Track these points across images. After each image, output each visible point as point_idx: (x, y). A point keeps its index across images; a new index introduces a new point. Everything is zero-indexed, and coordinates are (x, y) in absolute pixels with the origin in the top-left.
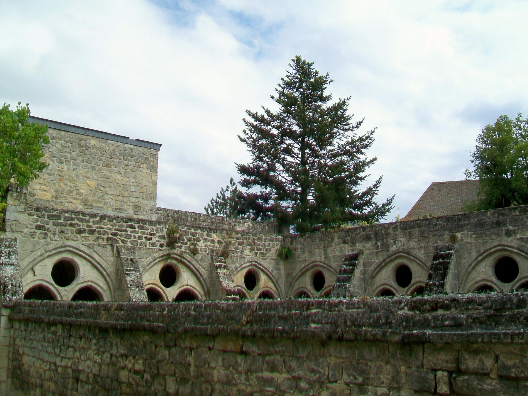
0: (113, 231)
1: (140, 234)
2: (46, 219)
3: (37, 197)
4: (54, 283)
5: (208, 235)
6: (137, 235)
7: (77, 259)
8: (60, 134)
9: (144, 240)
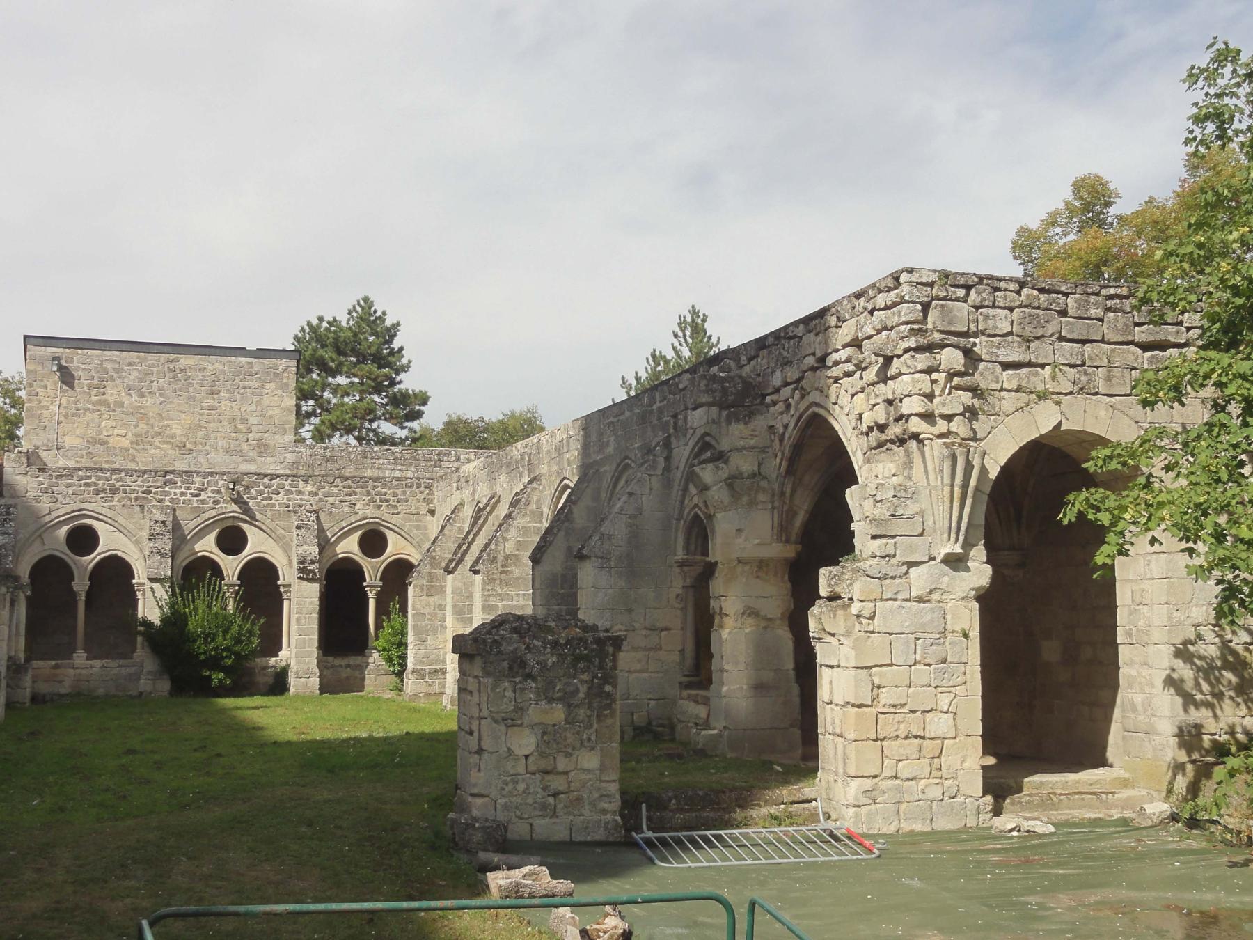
0: (145, 488)
1: (183, 490)
2: (54, 480)
3: (109, 445)
4: (68, 552)
5: (291, 485)
6: (178, 491)
7: (95, 524)
8: (138, 357)
9: (189, 497)
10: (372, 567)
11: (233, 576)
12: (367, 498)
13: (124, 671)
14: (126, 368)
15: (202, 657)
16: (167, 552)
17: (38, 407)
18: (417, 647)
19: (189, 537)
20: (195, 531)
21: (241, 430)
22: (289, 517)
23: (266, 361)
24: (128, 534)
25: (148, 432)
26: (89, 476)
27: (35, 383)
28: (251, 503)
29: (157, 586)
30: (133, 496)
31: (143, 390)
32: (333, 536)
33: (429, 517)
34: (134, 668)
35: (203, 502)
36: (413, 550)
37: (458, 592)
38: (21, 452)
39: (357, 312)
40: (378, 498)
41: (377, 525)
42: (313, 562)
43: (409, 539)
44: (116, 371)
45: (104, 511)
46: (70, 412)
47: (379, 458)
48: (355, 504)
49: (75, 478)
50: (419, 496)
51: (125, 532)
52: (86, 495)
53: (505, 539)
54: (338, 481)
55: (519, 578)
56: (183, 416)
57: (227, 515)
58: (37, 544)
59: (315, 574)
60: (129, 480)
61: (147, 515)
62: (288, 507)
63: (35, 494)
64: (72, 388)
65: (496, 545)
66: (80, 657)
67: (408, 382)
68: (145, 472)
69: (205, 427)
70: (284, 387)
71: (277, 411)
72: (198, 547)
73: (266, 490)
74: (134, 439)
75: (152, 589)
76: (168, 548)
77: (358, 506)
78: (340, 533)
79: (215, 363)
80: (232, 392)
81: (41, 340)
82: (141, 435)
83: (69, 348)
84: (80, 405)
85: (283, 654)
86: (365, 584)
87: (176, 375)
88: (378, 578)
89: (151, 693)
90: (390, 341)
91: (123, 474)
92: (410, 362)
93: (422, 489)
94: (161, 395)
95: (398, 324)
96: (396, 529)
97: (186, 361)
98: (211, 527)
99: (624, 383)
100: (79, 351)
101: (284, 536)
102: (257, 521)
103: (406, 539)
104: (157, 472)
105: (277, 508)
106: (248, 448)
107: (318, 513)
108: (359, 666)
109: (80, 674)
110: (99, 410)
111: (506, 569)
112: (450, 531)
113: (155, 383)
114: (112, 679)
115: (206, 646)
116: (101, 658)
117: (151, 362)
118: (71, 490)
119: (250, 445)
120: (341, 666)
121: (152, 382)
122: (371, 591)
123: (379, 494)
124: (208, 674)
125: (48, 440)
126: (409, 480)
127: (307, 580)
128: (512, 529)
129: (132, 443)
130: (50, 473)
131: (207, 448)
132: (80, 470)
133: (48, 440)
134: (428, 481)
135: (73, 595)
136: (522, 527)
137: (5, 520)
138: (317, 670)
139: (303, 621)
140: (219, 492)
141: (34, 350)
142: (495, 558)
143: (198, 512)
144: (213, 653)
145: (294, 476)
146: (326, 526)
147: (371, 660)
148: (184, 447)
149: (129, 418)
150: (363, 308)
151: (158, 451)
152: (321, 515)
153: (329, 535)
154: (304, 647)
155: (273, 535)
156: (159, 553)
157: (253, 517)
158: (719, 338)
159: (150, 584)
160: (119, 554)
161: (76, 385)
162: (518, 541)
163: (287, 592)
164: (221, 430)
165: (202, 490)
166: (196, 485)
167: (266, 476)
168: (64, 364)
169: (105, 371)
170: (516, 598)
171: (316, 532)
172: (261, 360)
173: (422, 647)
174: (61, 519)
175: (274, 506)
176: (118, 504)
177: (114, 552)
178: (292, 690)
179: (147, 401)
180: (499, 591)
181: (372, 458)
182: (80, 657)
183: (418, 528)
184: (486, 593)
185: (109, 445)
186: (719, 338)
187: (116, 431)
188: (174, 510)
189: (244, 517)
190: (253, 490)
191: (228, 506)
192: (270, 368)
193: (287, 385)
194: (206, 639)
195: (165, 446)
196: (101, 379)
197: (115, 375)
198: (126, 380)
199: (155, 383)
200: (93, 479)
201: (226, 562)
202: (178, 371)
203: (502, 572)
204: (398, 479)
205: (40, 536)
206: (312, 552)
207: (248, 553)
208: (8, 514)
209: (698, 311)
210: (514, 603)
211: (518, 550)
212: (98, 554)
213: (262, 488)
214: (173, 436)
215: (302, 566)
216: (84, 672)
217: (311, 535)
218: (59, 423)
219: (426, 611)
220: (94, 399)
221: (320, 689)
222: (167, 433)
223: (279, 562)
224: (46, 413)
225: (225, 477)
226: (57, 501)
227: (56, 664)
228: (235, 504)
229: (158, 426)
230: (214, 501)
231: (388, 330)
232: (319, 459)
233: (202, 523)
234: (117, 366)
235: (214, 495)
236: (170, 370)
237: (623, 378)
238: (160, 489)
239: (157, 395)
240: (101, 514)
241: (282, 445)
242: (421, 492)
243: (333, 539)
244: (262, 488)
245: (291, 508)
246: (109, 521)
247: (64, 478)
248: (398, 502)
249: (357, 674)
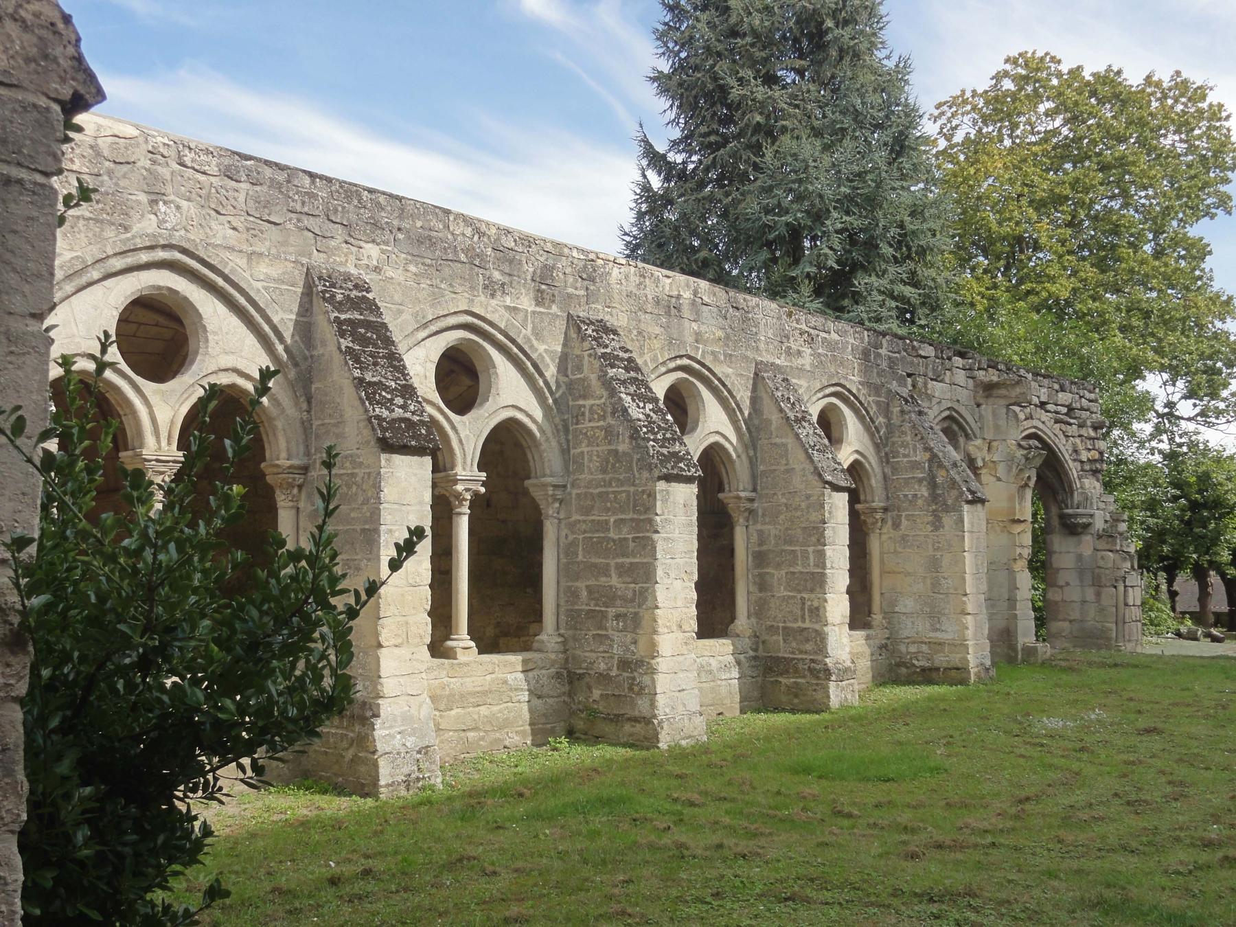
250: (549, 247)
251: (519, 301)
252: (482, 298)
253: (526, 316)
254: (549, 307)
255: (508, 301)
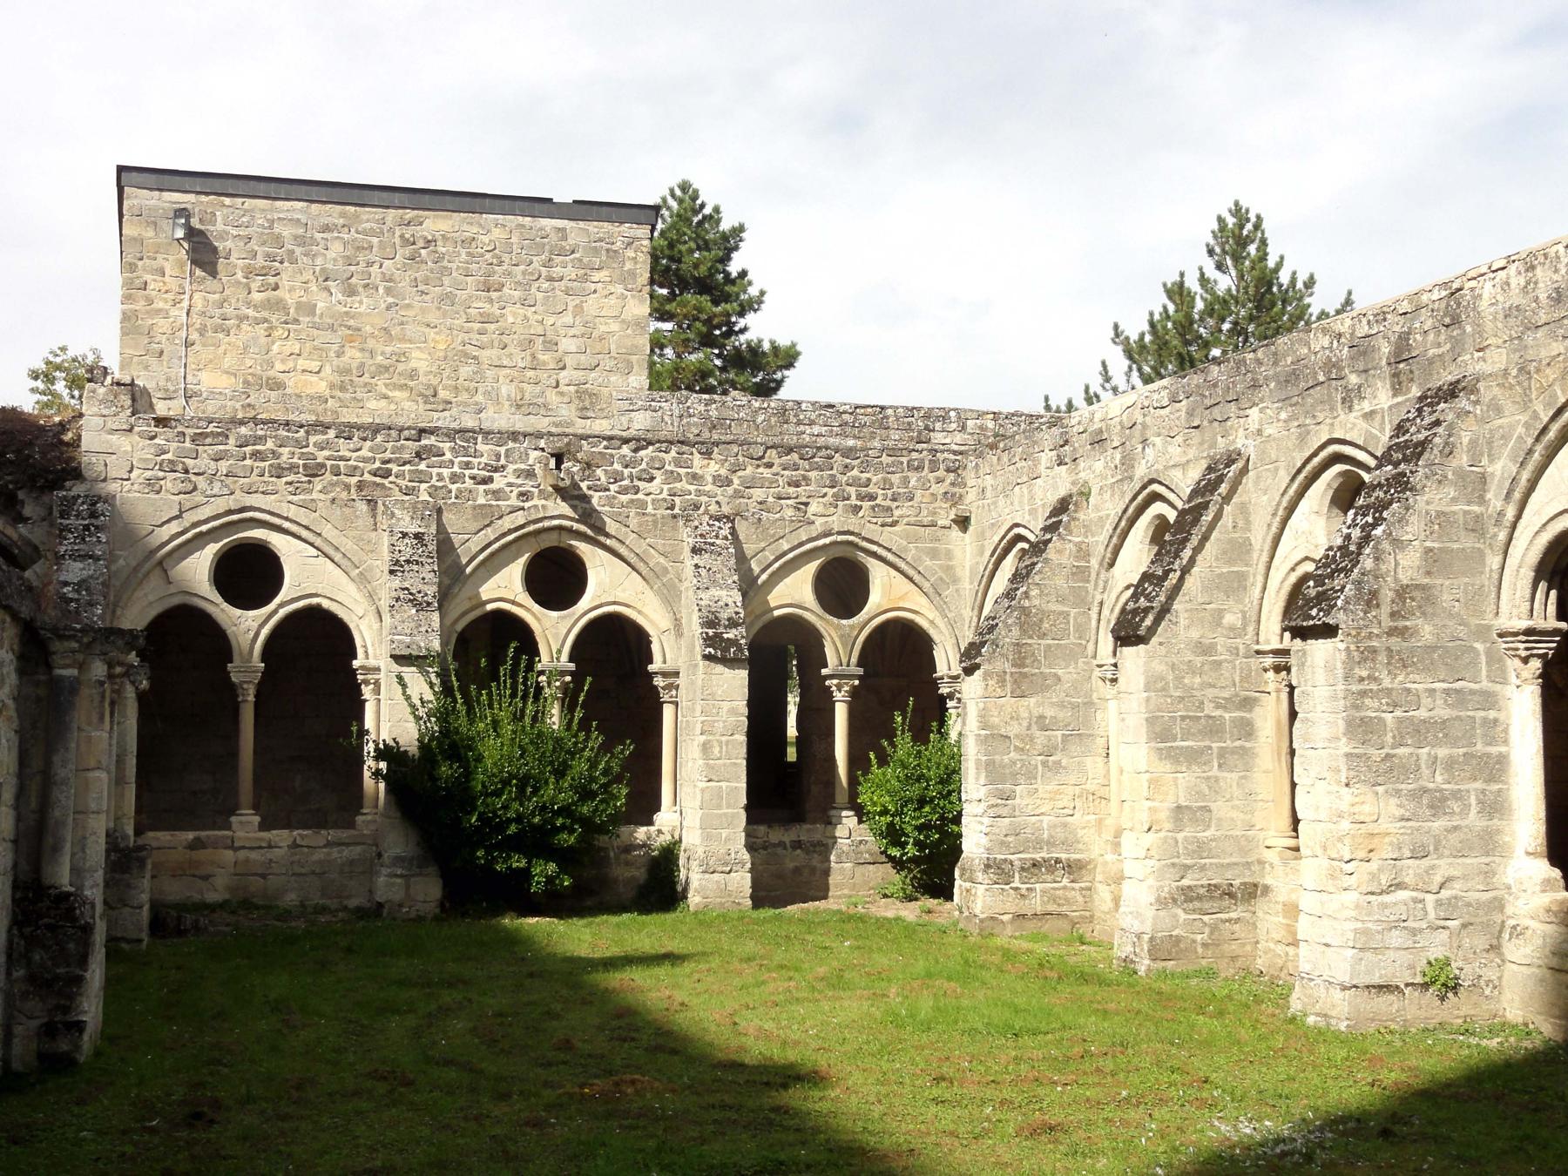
0: (377, 464)
1: (456, 469)
2: (188, 444)
3: (288, 391)
6: (446, 472)
7: (277, 541)
8: (343, 215)
9: (469, 483)
10: (841, 637)
11: (559, 652)
12: (831, 492)
13: (335, 853)
14: (318, 236)
15: (513, 829)
16: (429, 599)
17: (148, 312)
18: (991, 812)
19: (468, 570)
20: (481, 557)
21: (544, 363)
22: (675, 528)
23: (593, 227)
24: (344, 562)
25: (362, 365)
26: (260, 438)
27: (140, 263)
28: (596, 499)
29: (410, 673)
30: (354, 480)
31: (353, 280)
32: (763, 571)
33: (955, 532)
34: (359, 849)
35: (497, 494)
36: (924, 600)
37: (1159, 685)
38: (118, 384)
39: (669, 208)
40: (852, 490)
41: (850, 549)
42: (733, 623)
43: (917, 578)
44: (300, 241)
45: (292, 511)
46: (209, 322)
47: (812, 423)
48: (806, 504)
49: (232, 441)
50: (939, 489)
51: (338, 557)
52: (254, 478)
53: (1398, 544)
54: (772, 453)
55: (1431, 649)
56: (431, 333)
57: (547, 524)
58: (155, 580)
59: (740, 649)
60: (344, 448)
61: (384, 522)
62: (672, 508)
63: (149, 474)
64: (213, 273)
65: (1377, 559)
66: (246, 824)
67: (758, 329)
68: (376, 429)
69: (475, 358)
70: (626, 278)
71: (615, 327)
72: (489, 590)
73: (626, 472)
74: (336, 379)
75: (400, 678)
76: (432, 590)
77: (814, 507)
78: (777, 565)
79: (494, 229)
80: (526, 287)
81: (154, 177)
82: (348, 371)
83: (207, 194)
84: (229, 310)
85: (665, 819)
86: (824, 671)
87: (416, 251)
88: (854, 660)
89: (401, 906)
90: (726, 259)
91: (332, 433)
92: (762, 293)
93: (941, 473)
94: (388, 291)
95: (741, 228)
96: (890, 557)
97: (436, 224)
98: (513, 548)
99: (1117, 335)
100: (227, 201)
101: (666, 570)
102: (607, 535)
103: (911, 579)
104: (401, 430)
105: (650, 509)
106: (559, 399)
107: (733, 521)
108: (820, 843)
109: (247, 860)
110: (266, 320)
111: (1401, 624)
112: (1059, 552)
113: (376, 266)
114: (313, 873)
115: (521, 805)
116: (289, 826)
117: (368, 225)
118: (224, 466)
119: (562, 394)
120: (781, 844)
121: (370, 264)
122: (839, 688)
123: (854, 483)
124: (523, 864)
125: (168, 379)
126: (915, 455)
127: (724, 661)
128: (1413, 519)
129: (332, 386)
130: (180, 429)
131: (479, 398)
132: (242, 423)
133: (168, 379)
134: (952, 457)
135: (230, 691)
136: (1440, 514)
137: (86, 528)
138: (747, 856)
139: (716, 750)
140: (530, 474)
141: (138, 197)
142: (1374, 594)
143: (488, 516)
144: (536, 820)
145: (682, 443)
146: (749, 549)
147: (840, 831)
148: (435, 396)
149: (328, 336)
150: (681, 201)
151: (383, 403)
152: (742, 528)
153: (756, 569)
154: (719, 807)
155: (641, 566)
156: (413, 602)
157: (601, 530)
158: (1282, 258)
159: (396, 668)
160: (326, 604)
161: (220, 267)
162: (1430, 550)
163: (669, 687)
164: (505, 363)
165: (496, 470)
166: (484, 460)
167: (626, 441)
168: (198, 226)
169: (278, 241)
170: (1426, 701)
171: (733, 561)
172: (582, 224)
173: (1004, 811)
174: (204, 528)
175: (643, 505)
176: (322, 496)
177: (314, 601)
178: (694, 899)
179: (361, 302)
180: (1387, 683)
181: (799, 423)
182: (246, 824)
183: (934, 554)
184: (1354, 688)
185: (288, 391)
186: (1282, 258)
187: (302, 363)
188: (439, 511)
189: (582, 528)
190: (599, 472)
191: (550, 503)
192: (601, 240)
193: (632, 274)
194: (521, 789)
195: (397, 394)
196: (271, 258)
197: (298, 250)
198: (319, 261)
199: (376, 266)
200: (270, 444)
201: (547, 624)
202: (421, 243)
203: (1391, 632)
204: (893, 452)
205: (160, 563)
206: (730, 601)
207: (589, 605)
208: (93, 515)
209: (1247, 211)
210: (1422, 713)
211: (1428, 573)
212: (281, 605)
213: (617, 466)
214: (413, 374)
215: (711, 632)
216: (254, 855)
217: (723, 566)
218: (188, 344)
219: (1013, 730)
220: (257, 297)
221: (752, 897)
222: (401, 367)
223: (651, 622)
224: (162, 325)
225: (542, 443)
226: (195, 489)
227: (197, 839)
228: (564, 499)
229: (383, 353)
230: (521, 494)
231: (725, 237)
232: (695, 424)
233: (497, 539)
234: (301, 231)
235: (519, 481)
236: (407, 242)
237: (1116, 327)
238: (407, 467)
239: (381, 290)
240: (287, 519)
241: (625, 395)
242: (940, 481)
243: (764, 577)
244: (617, 466)
245: (677, 511)
246: (304, 533)
247: (209, 440)
248: (894, 500)
249: (816, 861)
250: (1405, 306)
251: (1376, 401)
252: (1343, 416)
253: (1383, 417)
254: (1409, 390)
255: (1366, 406)
